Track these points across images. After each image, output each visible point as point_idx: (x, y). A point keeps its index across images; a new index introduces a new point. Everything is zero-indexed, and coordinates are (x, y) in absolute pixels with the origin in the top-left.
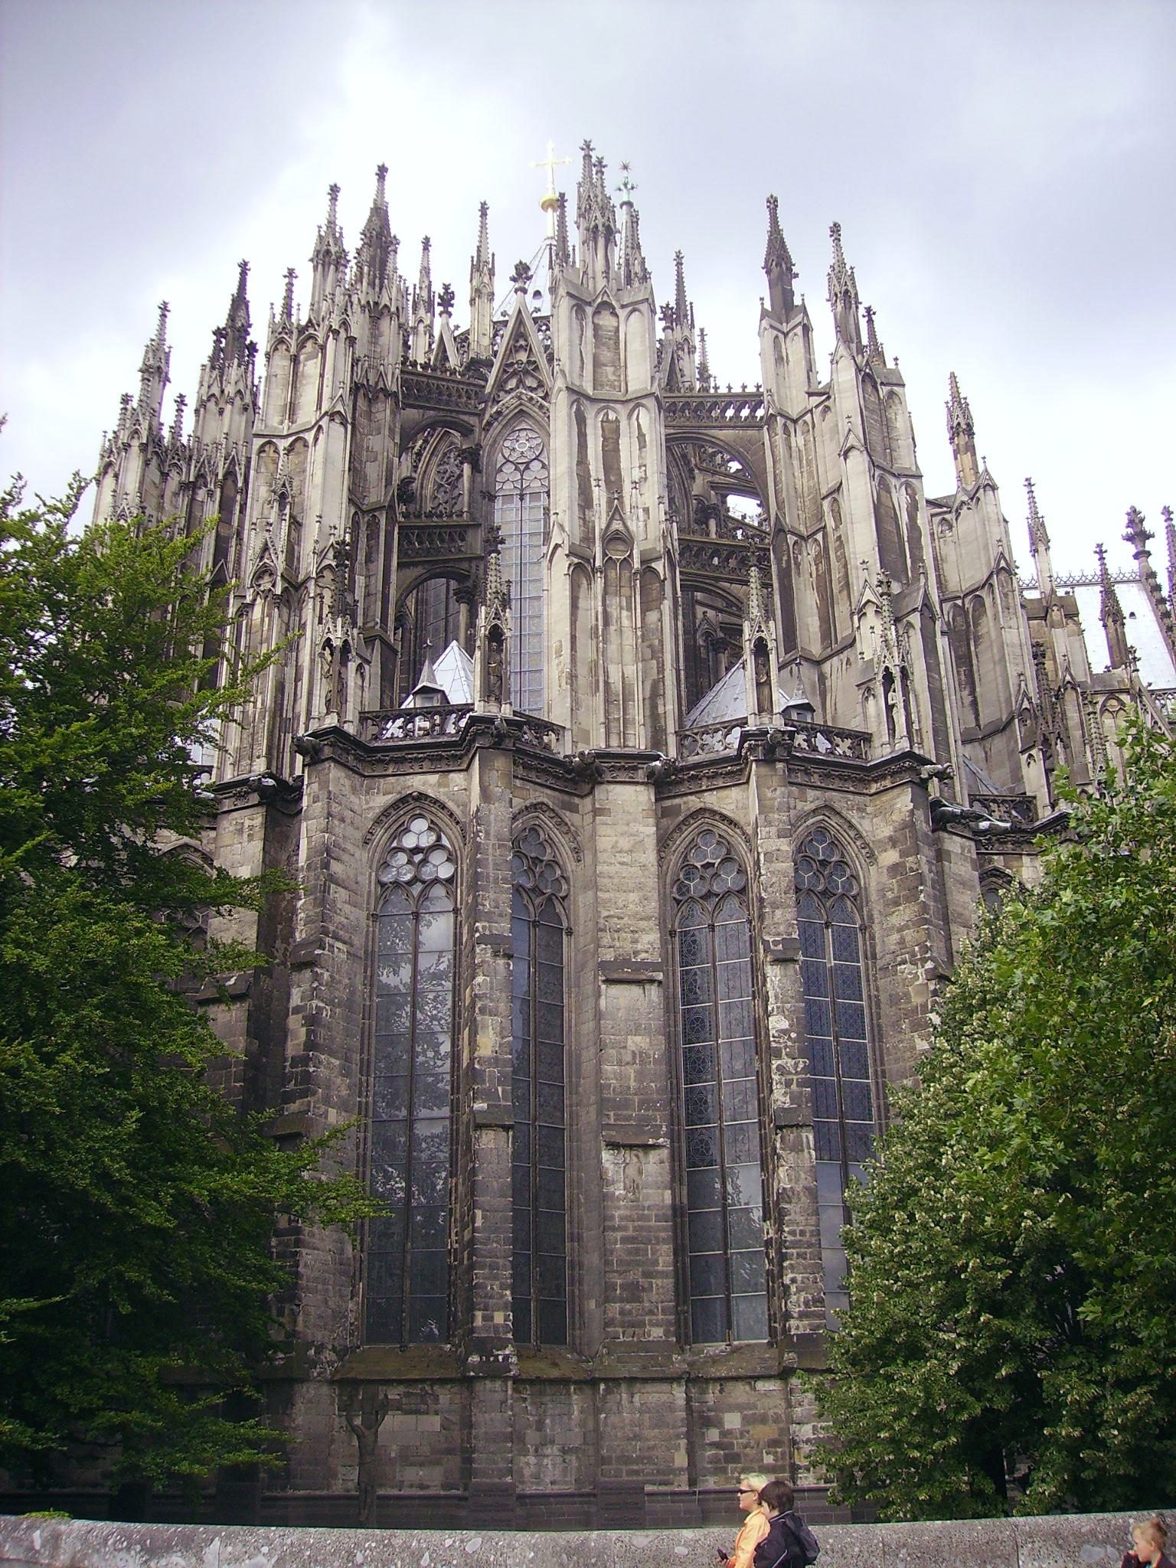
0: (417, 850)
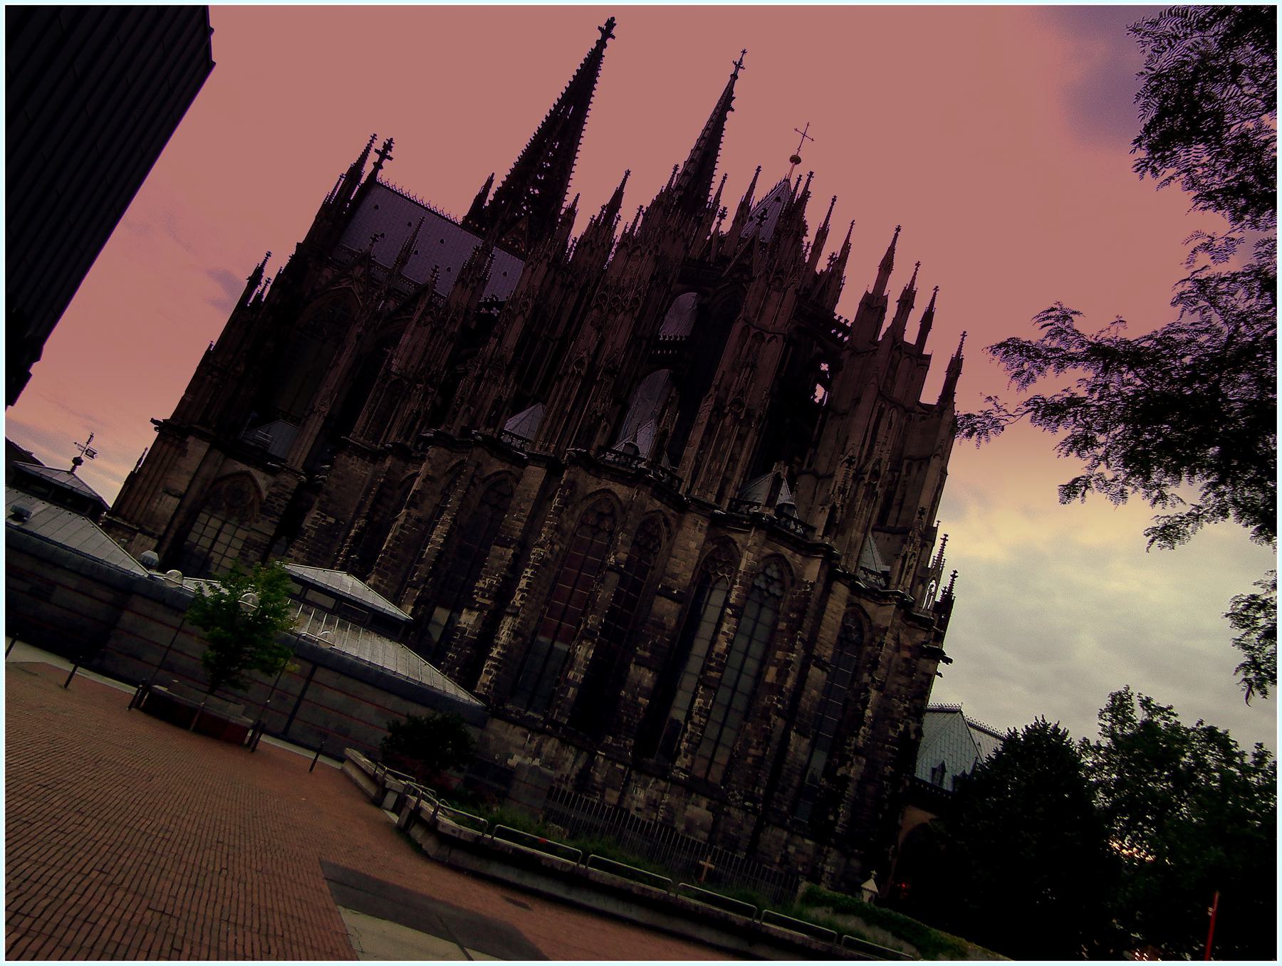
0: (772, 578)
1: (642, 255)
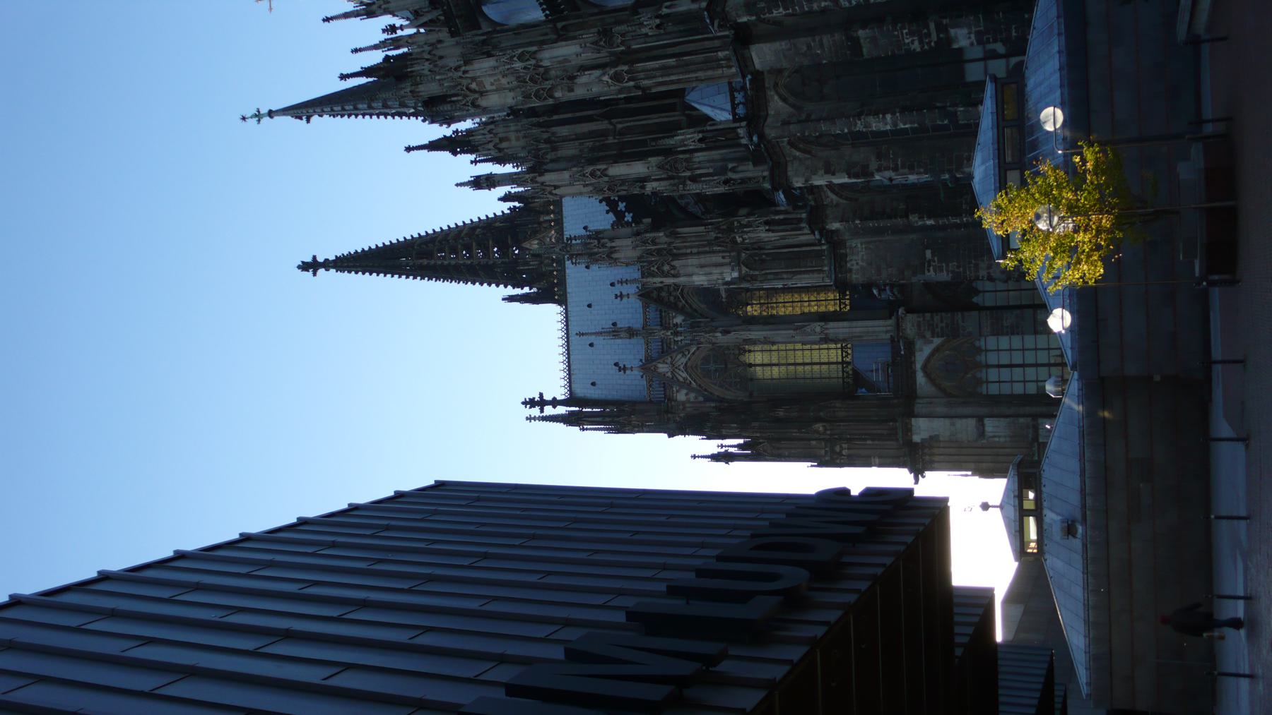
1: (473, 79)
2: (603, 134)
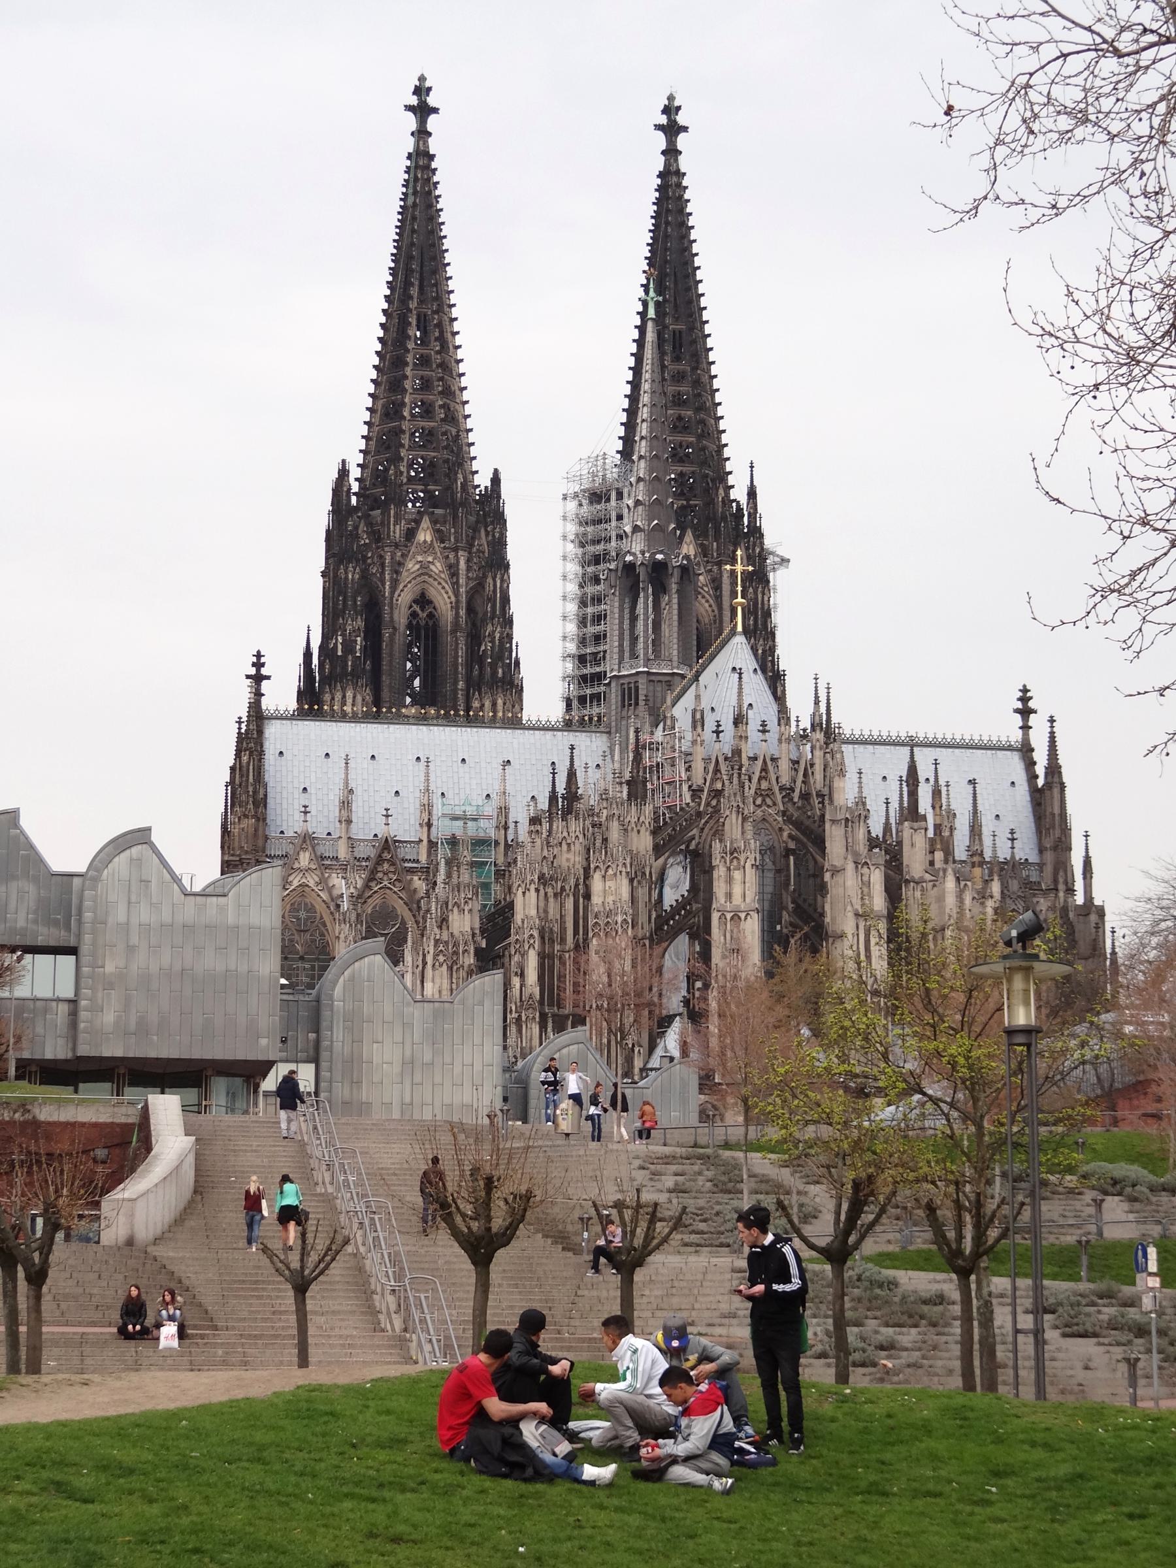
2: (563, 940)
